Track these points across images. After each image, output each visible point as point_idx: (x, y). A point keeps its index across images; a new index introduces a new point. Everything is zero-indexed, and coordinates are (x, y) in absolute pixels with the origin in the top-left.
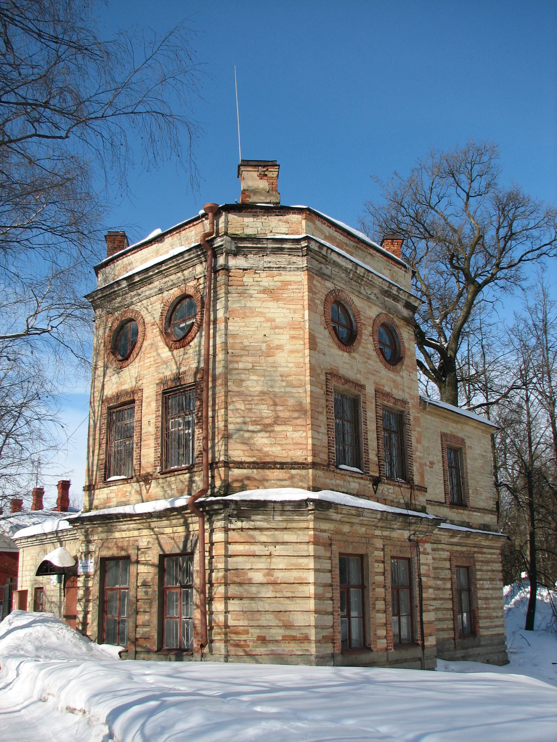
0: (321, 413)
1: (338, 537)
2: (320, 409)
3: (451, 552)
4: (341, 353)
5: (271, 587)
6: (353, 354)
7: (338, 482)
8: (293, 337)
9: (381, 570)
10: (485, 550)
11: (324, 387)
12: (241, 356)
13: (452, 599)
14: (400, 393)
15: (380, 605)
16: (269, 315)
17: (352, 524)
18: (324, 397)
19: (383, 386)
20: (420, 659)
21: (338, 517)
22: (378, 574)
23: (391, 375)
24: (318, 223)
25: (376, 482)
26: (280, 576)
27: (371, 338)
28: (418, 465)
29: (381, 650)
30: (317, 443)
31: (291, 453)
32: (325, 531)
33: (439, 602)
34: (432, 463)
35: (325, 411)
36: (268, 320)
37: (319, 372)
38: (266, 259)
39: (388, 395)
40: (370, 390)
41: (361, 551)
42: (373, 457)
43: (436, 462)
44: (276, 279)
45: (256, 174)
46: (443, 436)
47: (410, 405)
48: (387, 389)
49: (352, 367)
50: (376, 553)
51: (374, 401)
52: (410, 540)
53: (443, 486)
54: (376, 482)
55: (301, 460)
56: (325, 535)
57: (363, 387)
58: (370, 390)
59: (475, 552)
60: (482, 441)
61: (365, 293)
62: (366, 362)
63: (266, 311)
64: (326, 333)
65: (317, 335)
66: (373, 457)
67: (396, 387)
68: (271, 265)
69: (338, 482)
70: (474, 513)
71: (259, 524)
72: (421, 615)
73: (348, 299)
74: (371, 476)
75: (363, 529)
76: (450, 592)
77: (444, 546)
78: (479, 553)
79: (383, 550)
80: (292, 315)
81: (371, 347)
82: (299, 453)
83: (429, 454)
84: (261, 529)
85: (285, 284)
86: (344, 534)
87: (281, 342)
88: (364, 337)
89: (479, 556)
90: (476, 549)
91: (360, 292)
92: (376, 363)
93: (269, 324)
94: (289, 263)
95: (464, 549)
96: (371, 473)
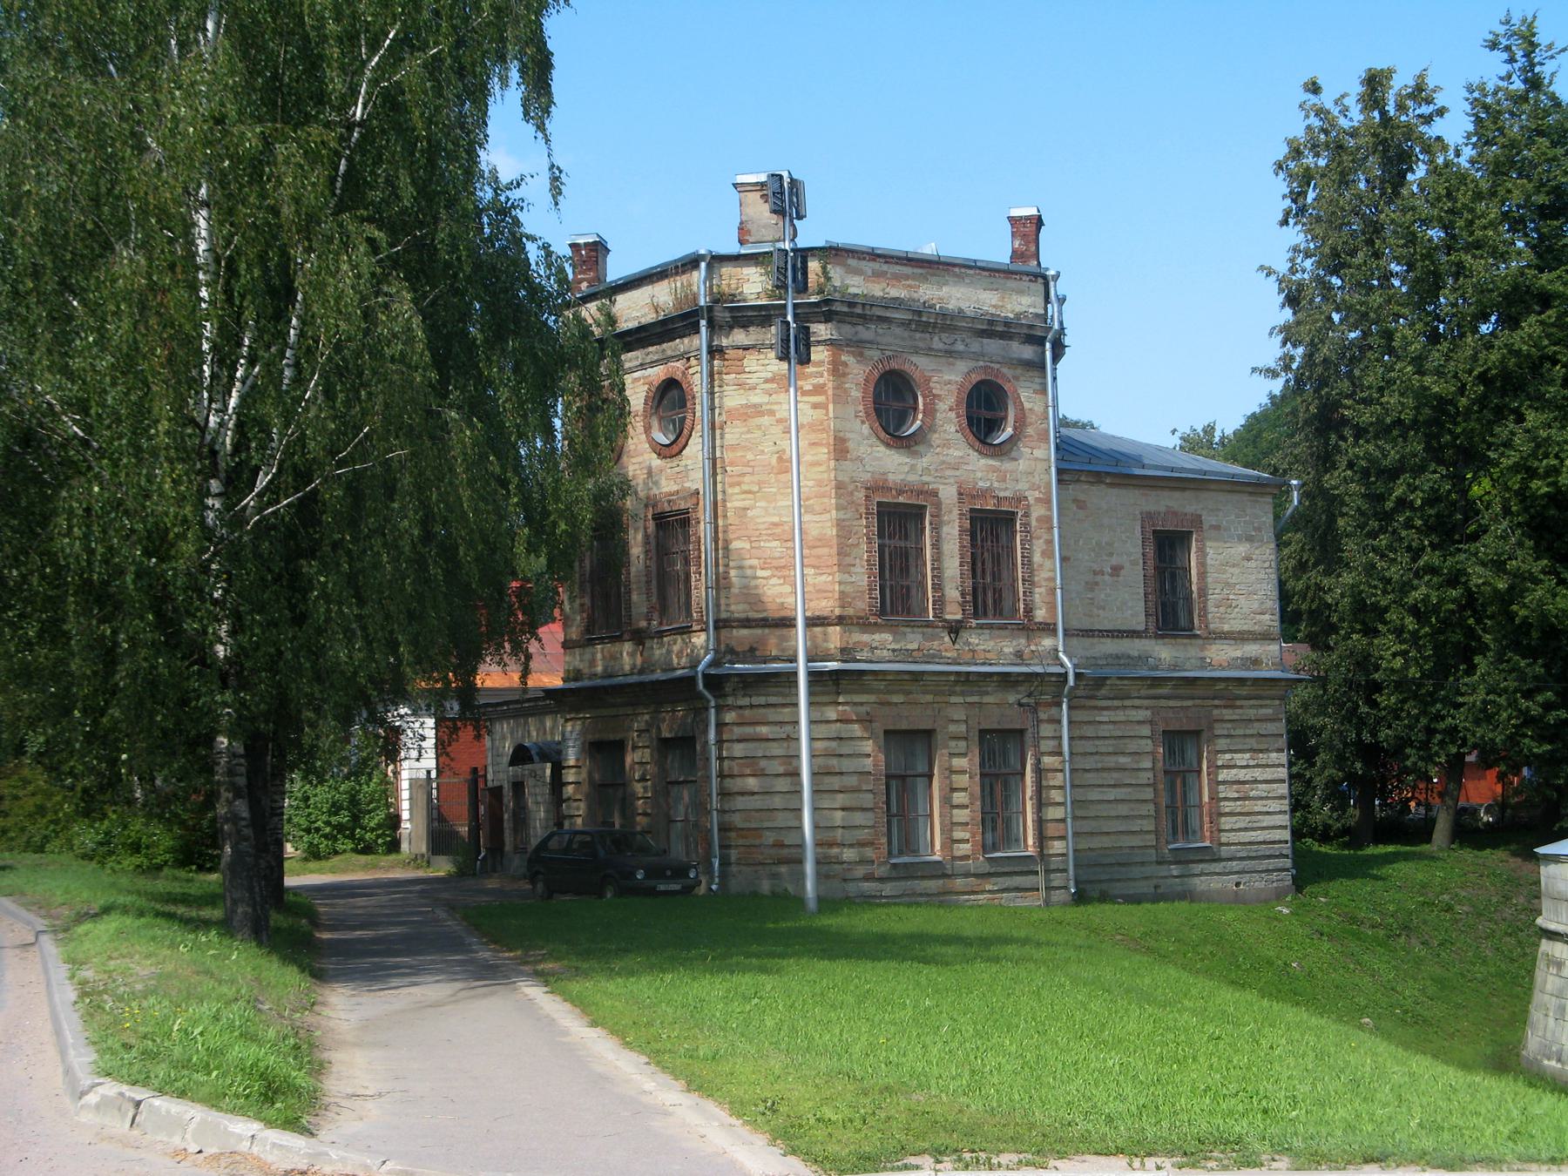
10: (1238, 703)
11: (863, 510)
12: (744, 474)
13: (1154, 785)
21: (882, 685)
24: (852, 262)
25: (955, 629)
30: (848, 589)
32: (862, 704)
34: (1116, 570)
36: (779, 421)
37: (851, 487)
39: (983, 494)
40: (948, 494)
41: (929, 727)
43: (1127, 565)
46: (1147, 517)
49: (913, 467)
50: (952, 728)
51: (956, 512)
52: (1020, 705)
56: (863, 709)
59: (1217, 707)
61: (941, 346)
63: (775, 407)
64: (866, 429)
65: (848, 435)
71: (772, 700)
74: (946, 621)
75: (929, 698)
76: (1150, 775)
77: (1137, 702)
79: (966, 721)
82: (824, 603)
83: (1111, 554)
89: (1228, 714)
90: (1216, 702)
91: (930, 349)
95: (1190, 703)
96: (948, 617)
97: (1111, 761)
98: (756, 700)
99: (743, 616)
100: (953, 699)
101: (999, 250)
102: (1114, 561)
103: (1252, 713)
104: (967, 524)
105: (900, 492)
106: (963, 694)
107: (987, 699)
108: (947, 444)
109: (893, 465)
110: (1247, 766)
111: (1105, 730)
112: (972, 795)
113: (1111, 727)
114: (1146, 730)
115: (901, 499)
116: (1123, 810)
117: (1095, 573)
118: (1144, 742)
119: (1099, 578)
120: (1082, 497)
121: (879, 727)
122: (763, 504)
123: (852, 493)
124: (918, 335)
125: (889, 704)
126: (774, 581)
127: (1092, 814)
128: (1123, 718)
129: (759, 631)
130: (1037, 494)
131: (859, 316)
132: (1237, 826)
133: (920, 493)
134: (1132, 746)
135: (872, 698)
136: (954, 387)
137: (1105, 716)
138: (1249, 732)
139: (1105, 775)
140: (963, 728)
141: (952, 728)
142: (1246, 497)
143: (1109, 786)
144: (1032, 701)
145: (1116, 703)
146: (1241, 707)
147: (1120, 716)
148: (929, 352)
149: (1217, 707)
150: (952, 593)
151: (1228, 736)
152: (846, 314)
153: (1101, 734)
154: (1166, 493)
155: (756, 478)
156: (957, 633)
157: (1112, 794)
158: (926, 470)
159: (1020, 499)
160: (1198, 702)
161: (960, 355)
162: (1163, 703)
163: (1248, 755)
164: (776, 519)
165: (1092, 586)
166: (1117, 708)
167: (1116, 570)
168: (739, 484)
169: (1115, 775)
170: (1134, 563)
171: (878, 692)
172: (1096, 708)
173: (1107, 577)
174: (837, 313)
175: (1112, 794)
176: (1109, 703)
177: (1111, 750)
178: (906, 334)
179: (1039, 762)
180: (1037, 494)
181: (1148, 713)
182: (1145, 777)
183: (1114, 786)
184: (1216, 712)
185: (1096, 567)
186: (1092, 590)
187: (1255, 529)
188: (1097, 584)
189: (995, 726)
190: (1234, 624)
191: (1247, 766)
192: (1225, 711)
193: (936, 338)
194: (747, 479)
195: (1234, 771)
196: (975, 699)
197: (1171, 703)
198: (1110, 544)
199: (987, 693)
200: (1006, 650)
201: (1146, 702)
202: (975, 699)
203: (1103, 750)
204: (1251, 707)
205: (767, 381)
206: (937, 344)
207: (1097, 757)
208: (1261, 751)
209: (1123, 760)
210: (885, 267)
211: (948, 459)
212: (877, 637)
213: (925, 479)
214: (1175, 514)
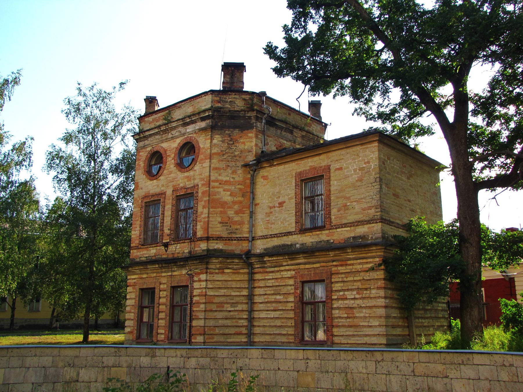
0: (137, 220)
3: (297, 271)
4: (152, 182)
10: (349, 262)
22: (163, 297)
23: (186, 174)
25: (166, 245)
28: (202, 223)
33: (278, 313)
34: (281, 204)
39: (182, 188)
43: (287, 201)
47: (200, 186)
49: (158, 186)
53: (294, 218)
54: (166, 245)
56: (134, 281)
58: (169, 192)
59: (336, 266)
60: (361, 155)
64: (144, 177)
65: (139, 181)
69: (144, 252)
70: (338, 230)
75: (155, 275)
77: (287, 268)
78: (342, 265)
81: (172, 166)
83: (279, 197)
88: (168, 163)
89: (341, 269)
90: (334, 263)
95: (318, 265)
96: (164, 241)
97: (272, 298)
100: (163, 274)
102: (280, 200)
103: (359, 267)
104: (174, 202)
105: (153, 196)
106: (165, 272)
107: (175, 273)
108: (171, 173)
110: (355, 299)
111: (270, 283)
112: (166, 315)
113: (273, 281)
114: (291, 282)
116: (278, 323)
117: (271, 208)
118: (289, 288)
119: (272, 210)
120: (266, 174)
121: (137, 287)
124: (164, 135)
127: (262, 324)
128: (280, 276)
132: (348, 333)
134: (284, 290)
137: (270, 276)
138: (355, 278)
139: (269, 305)
140: (165, 286)
142: (359, 148)
143: (272, 310)
145: (276, 269)
146: (353, 264)
147: (278, 275)
148: (167, 140)
149: (336, 266)
150: (167, 231)
151: (343, 282)
153: (268, 285)
154: (310, 160)
156: (167, 247)
157: (272, 314)
158: (163, 186)
160: (322, 264)
161: (177, 137)
162: (302, 266)
163: (355, 293)
165: (268, 214)
166: (278, 271)
167: (281, 204)
169: (274, 305)
170: (290, 199)
171: (137, 274)
172: (267, 272)
173: (276, 208)
175: (272, 314)
176: (273, 269)
177: (272, 292)
180: (202, 182)
181: (293, 273)
182: (290, 306)
183: (275, 310)
184: (334, 269)
185: (271, 205)
186: (269, 216)
187: (365, 163)
188: (271, 213)
190: (351, 218)
191: (355, 299)
192: (340, 268)
195: (346, 302)
197: (307, 266)
198: (279, 192)
199: (174, 271)
200: (186, 251)
201: (292, 267)
202: (170, 274)
203: (268, 292)
204: (360, 264)
206: (170, 136)
207: (266, 296)
208: (366, 289)
209: (278, 297)
211: (170, 179)
212: (141, 253)
213: (162, 188)
214: (315, 168)
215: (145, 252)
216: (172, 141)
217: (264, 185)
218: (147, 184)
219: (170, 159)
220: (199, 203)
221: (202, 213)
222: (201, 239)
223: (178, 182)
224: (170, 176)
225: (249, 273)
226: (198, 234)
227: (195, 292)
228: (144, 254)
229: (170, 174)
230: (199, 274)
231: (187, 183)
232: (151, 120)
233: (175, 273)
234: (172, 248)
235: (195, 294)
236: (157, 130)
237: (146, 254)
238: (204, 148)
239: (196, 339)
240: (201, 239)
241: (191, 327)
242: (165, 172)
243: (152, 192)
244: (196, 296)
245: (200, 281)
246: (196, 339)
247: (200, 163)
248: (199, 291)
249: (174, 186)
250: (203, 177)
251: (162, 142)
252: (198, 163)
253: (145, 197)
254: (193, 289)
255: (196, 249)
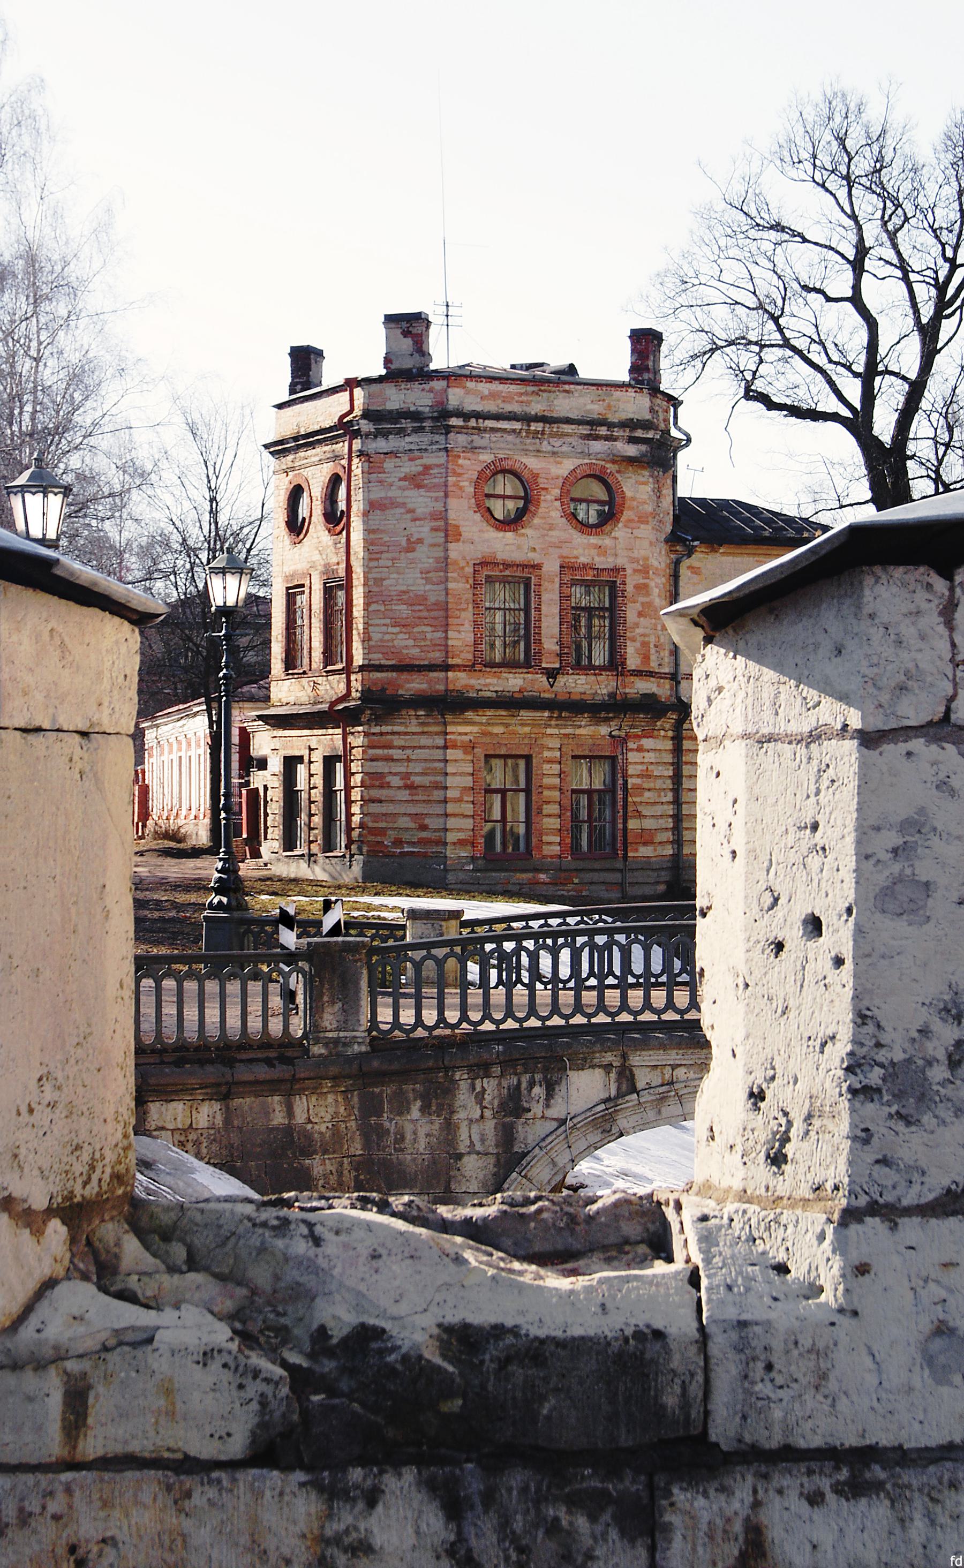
1: (487, 740)
2: (464, 606)
4: (501, 534)
5: (408, 792)
6: (523, 531)
7: (488, 681)
8: (435, 529)
9: (557, 772)
11: (471, 581)
14: (610, 559)
15: (554, 809)
16: (410, 506)
17: (507, 725)
18: (471, 591)
19: (577, 558)
20: (621, 871)
23: (593, 540)
25: (552, 674)
26: (417, 780)
27: (558, 503)
28: (638, 644)
29: (552, 857)
31: (429, 655)
32: (466, 734)
35: (471, 606)
37: (462, 564)
38: (408, 439)
39: (584, 567)
40: (551, 567)
42: (550, 644)
44: (418, 462)
45: (399, 331)
47: (629, 571)
48: (583, 560)
49: (519, 547)
50: (547, 754)
51: (557, 580)
54: (552, 674)
55: (439, 662)
57: (538, 567)
58: (551, 567)
61: (550, 448)
62: (543, 536)
63: (408, 500)
65: (462, 523)
66: (550, 644)
67: (604, 554)
68: (412, 447)
69: (488, 681)
71: (397, 729)
72: (625, 822)
73: (517, 465)
75: (527, 729)
80: (434, 504)
82: (438, 654)
84: (398, 733)
85: (427, 468)
86: (497, 735)
87: (422, 535)
88: (543, 504)
92: (565, 532)
93: (409, 516)
94: (432, 444)
96: (544, 665)
98: (385, 729)
99: (377, 663)
100: (549, 731)
101: (616, 364)
105: (507, 565)
107: (578, 731)
109: (506, 546)
115: (507, 573)
122: (394, 576)
123: (463, 568)
124: (528, 441)
125: (491, 734)
126: (401, 636)
129: (389, 674)
130: (635, 566)
131: (473, 428)
133: (524, 566)
135: (475, 729)
136: (561, 481)
141: (547, 754)
144: (623, 734)
152: (462, 427)
155: (389, 555)
159: (617, 570)
161: (566, 455)
164: (404, 588)
168: (377, 559)
174: (454, 427)
178: (518, 440)
179: (626, 783)
180: (635, 566)
189: (587, 753)
193: (545, 443)
194: (384, 556)
196: (569, 731)
199: (580, 727)
202: (569, 731)
205: (400, 480)
206: (545, 446)
210: (501, 387)
211: (553, 540)
212: (482, 681)
213: (531, 555)
215: (495, 681)
216: (552, 460)
217: (694, 584)
218: (486, 536)
219: (549, 497)
220: (630, 605)
221: (637, 625)
222: (638, 673)
223: (575, 552)
224: (551, 533)
225: (673, 738)
226: (628, 662)
227: (631, 770)
228: (490, 684)
229: (550, 529)
230: (638, 737)
231: (597, 559)
232: (486, 393)
233: (578, 731)
234: (561, 680)
235: (630, 772)
236: (517, 425)
237: (495, 685)
238: (633, 499)
239: (637, 850)
240: (638, 673)
241: (625, 828)
242: (536, 521)
243: (500, 556)
244: (632, 776)
245: (640, 749)
246: (637, 850)
247: (625, 526)
248: (640, 767)
249: (561, 557)
250: (636, 555)
251: (526, 452)
252: (620, 525)
253: (484, 564)
254: (626, 763)
255: (627, 691)
